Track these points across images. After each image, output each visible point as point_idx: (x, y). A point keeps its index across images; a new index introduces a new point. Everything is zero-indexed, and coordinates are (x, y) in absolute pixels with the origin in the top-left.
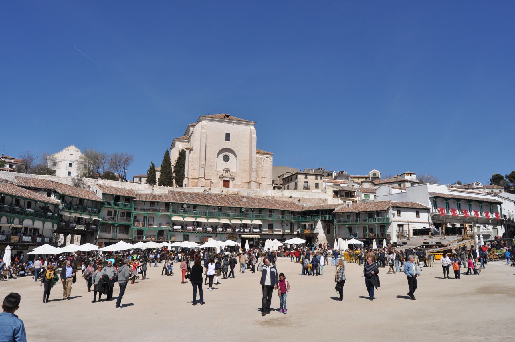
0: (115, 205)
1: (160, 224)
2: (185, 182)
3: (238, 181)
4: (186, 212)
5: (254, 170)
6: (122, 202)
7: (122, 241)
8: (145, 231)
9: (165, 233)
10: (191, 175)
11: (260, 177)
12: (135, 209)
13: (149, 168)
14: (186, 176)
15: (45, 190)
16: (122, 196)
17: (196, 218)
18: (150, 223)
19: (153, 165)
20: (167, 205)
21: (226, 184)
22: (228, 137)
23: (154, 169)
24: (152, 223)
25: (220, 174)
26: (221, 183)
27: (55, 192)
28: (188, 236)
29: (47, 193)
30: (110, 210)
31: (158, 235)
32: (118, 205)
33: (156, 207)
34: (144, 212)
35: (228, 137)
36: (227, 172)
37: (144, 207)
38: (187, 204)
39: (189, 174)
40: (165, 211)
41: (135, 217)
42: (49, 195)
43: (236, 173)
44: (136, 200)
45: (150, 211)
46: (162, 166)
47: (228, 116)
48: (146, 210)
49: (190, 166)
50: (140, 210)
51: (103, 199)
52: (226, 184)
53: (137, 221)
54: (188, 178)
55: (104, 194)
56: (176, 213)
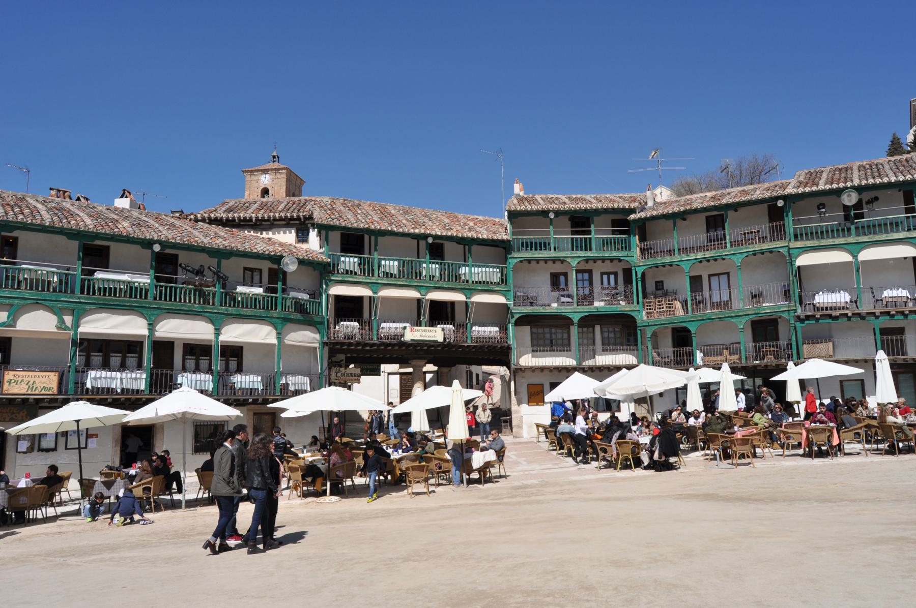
0: (575, 245)
1: (756, 296)
4: (871, 228)
6: (597, 234)
7: (577, 374)
8: (692, 328)
9: (782, 329)
12: (646, 252)
16: (597, 212)
18: (716, 299)
20: (775, 210)
24: (725, 298)
28: (901, 331)
30: (558, 268)
31: (755, 340)
32: (587, 246)
33: (731, 232)
34: (676, 258)
37: (676, 240)
38: (859, 189)
40: (773, 239)
41: (659, 285)
42: (303, 237)
44: (643, 215)
45: (705, 248)
48: (684, 250)
50: (671, 252)
51: (514, 233)
53: (666, 294)
55: (514, 216)
56: (818, 237)
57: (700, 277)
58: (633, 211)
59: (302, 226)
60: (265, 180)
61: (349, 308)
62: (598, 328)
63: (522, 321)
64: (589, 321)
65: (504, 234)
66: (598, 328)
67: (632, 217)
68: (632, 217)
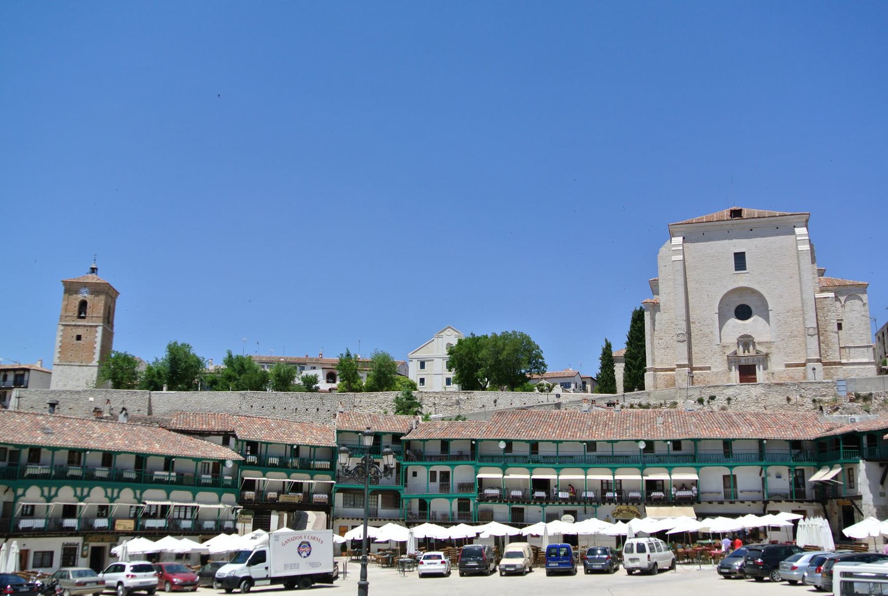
2: (648, 378)
3: (777, 365)
5: (811, 331)
10: (662, 362)
11: (837, 347)
13: (601, 352)
14: (649, 365)
15: (218, 433)
17: (531, 470)
19: (609, 346)
21: (747, 373)
22: (740, 260)
23: (610, 356)
25: (729, 352)
26: (735, 374)
27: (235, 436)
29: (220, 438)
35: (740, 260)
36: (746, 346)
39: (657, 360)
43: (769, 344)
44: (408, 437)
46: (627, 344)
47: (736, 214)
49: (656, 342)
52: (747, 373)
54: (656, 370)
57: (435, 472)
58: (403, 434)
59: (226, 437)
60: (84, 295)
61: (250, 485)
62: (380, 496)
63: (340, 490)
64: (375, 493)
65: (333, 443)
66: (380, 496)
67: (403, 438)
68: (403, 438)
